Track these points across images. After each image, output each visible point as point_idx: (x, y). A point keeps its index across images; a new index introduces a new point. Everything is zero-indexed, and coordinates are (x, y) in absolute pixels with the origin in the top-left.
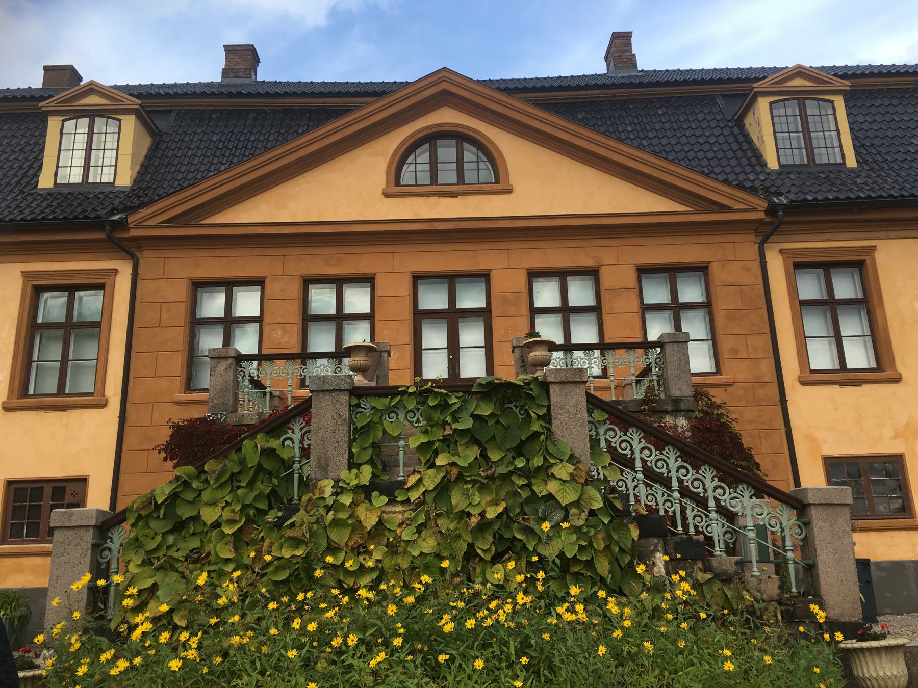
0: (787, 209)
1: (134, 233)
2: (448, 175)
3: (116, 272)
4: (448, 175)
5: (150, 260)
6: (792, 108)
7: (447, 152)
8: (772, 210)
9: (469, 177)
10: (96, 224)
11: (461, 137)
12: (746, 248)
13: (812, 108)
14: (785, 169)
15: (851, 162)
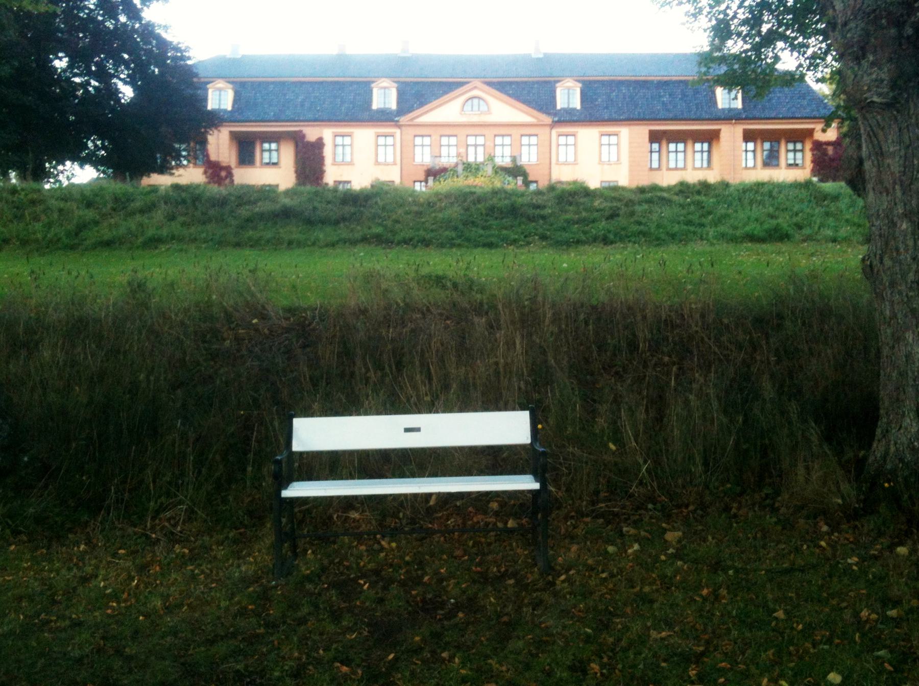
0: (556, 122)
1: (401, 123)
2: (476, 108)
3: (395, 133)
4: (476, 108)
5: (403, 128)
6: (566, 91)
7: (476, 101)
8: (553, 122)
9: (481, 108)
10: (392, 121)
11: (479, 98)
12: (547, 129)
13: (571, 91)
14: (561, 109)
15: (579, 107)
